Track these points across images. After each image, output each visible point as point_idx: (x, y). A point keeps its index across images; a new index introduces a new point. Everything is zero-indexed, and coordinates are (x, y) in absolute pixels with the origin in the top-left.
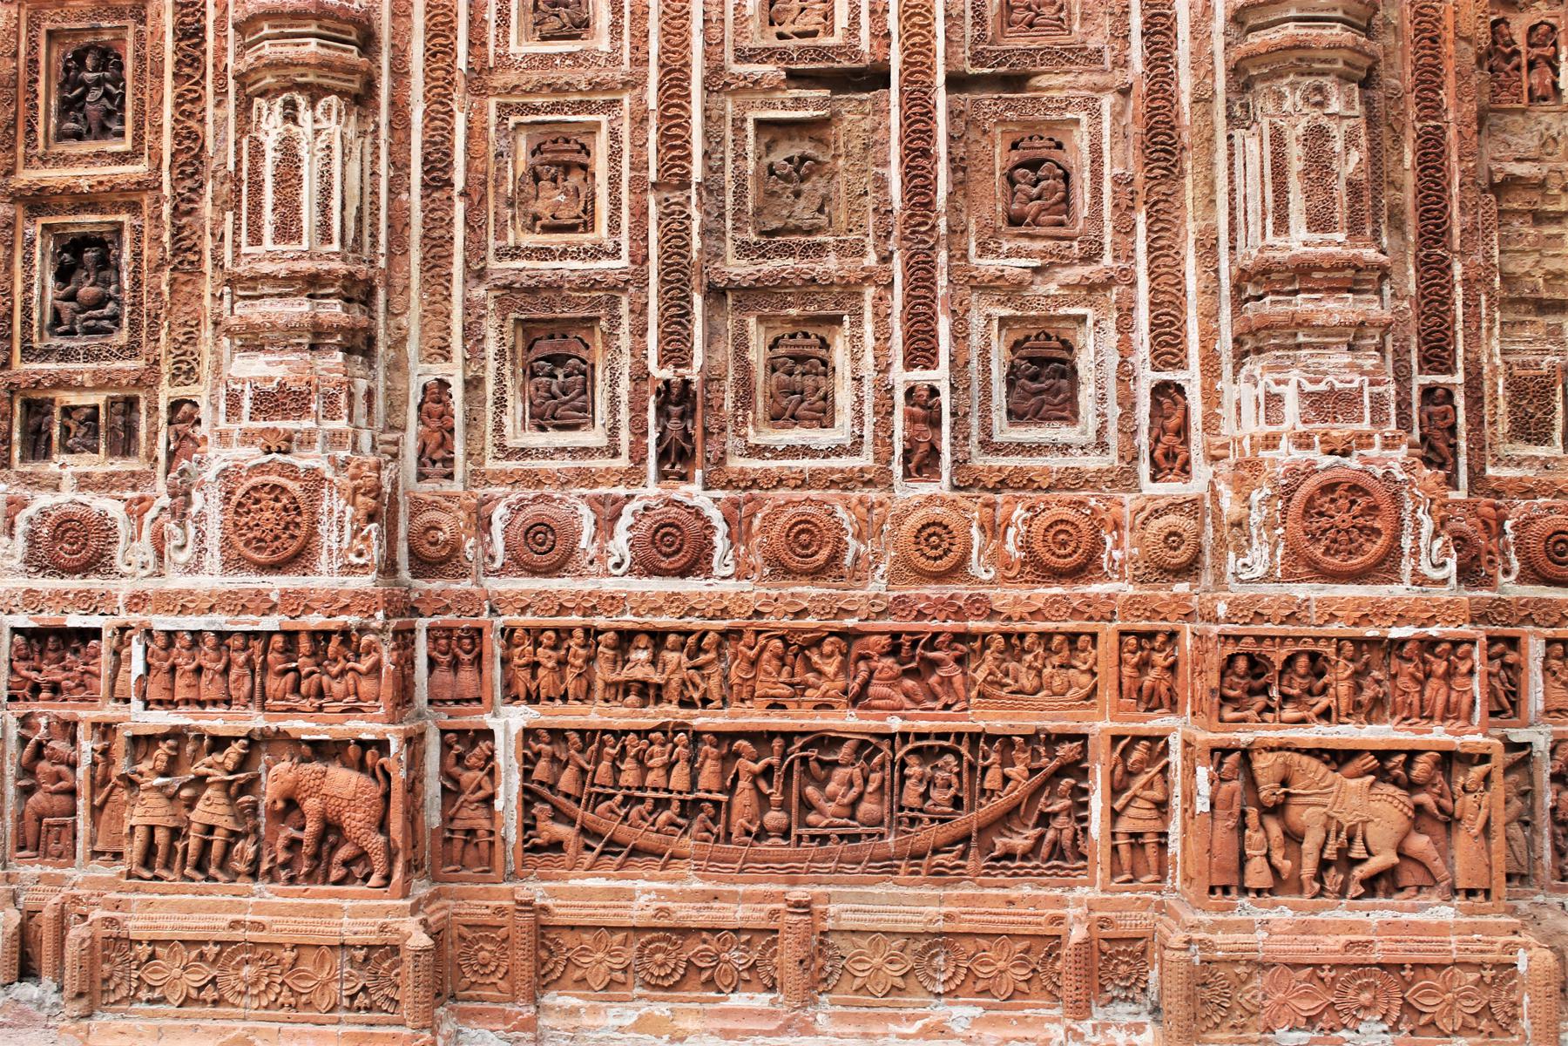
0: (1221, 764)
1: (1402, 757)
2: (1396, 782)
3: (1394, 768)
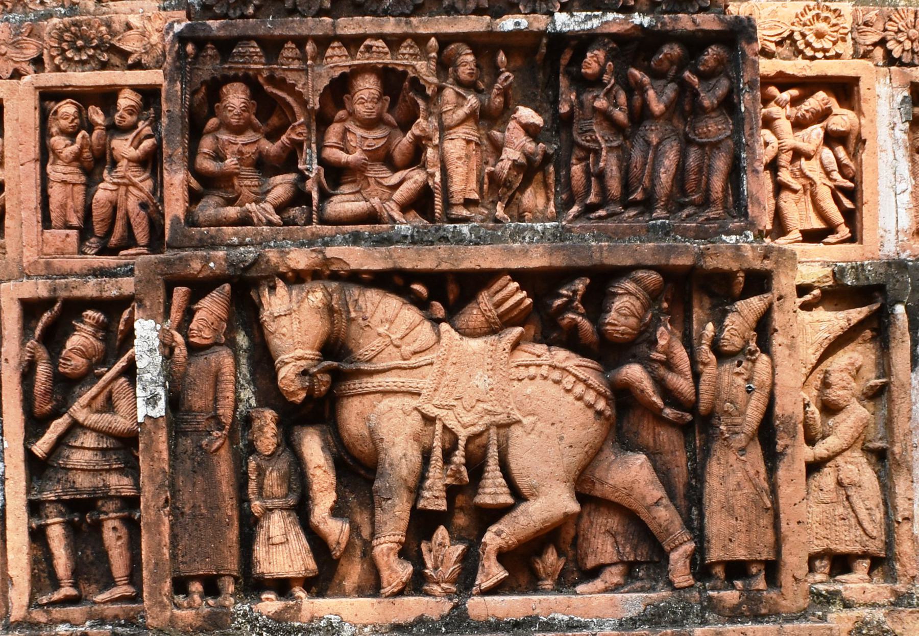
0: (189, 314)
1: (580, 285)
2: (571, 341)
3: (567, 307)
